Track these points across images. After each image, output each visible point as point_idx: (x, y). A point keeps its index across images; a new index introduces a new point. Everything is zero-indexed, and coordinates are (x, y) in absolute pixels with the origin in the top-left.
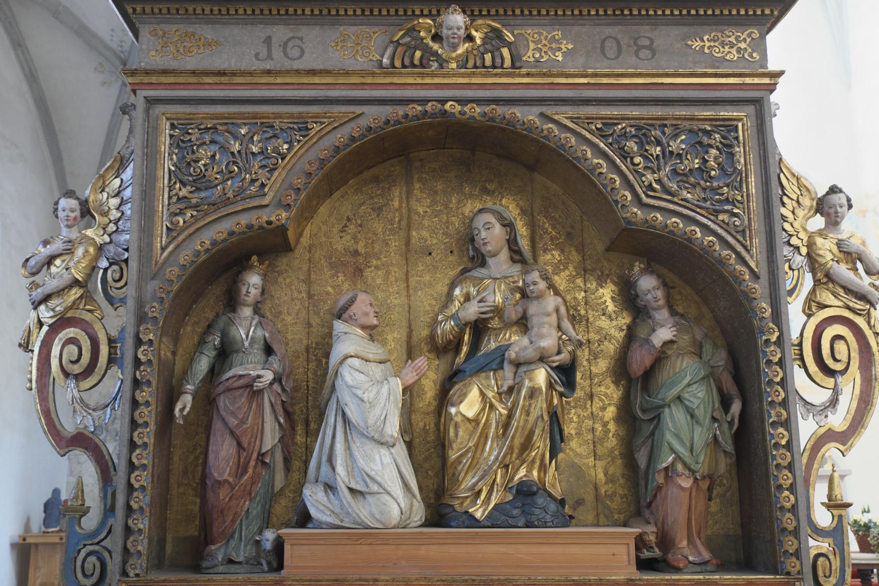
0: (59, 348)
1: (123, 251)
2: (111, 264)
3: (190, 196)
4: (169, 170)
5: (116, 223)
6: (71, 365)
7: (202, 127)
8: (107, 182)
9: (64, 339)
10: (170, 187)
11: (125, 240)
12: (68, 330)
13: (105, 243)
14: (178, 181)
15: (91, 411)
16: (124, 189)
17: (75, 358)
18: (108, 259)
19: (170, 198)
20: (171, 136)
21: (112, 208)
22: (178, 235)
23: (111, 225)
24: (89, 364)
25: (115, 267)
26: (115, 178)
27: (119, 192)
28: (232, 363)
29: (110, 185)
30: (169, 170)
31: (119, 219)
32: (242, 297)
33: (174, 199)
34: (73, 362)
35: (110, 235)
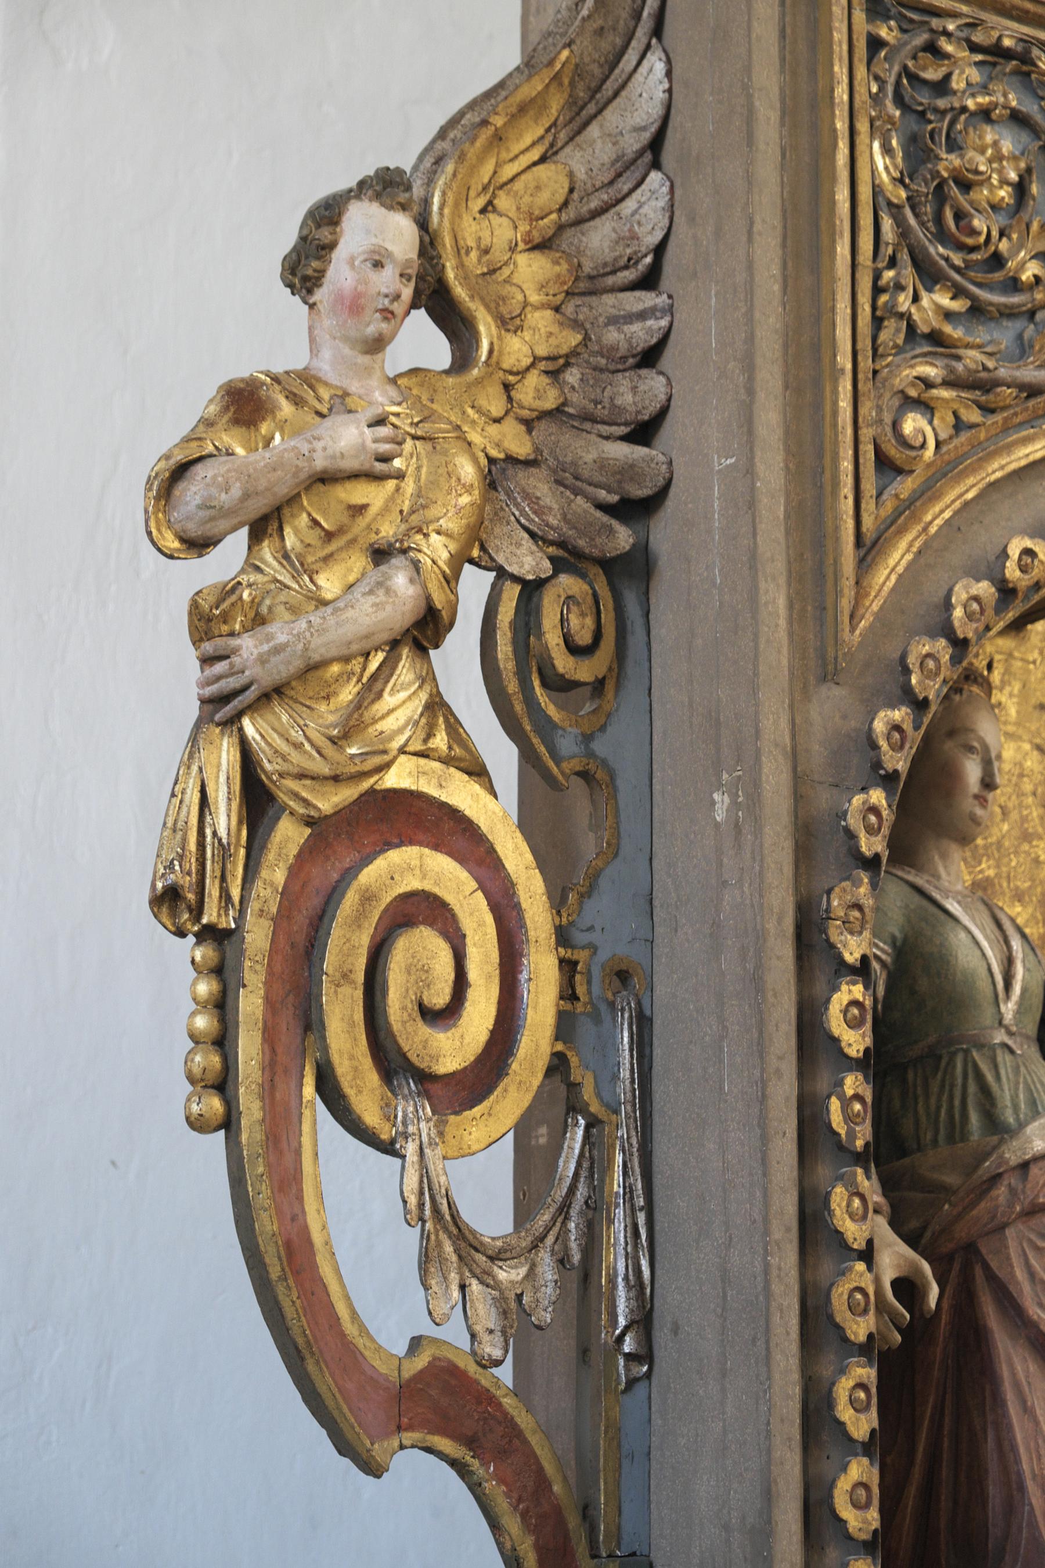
0: (364, 940)
1: (605, 518)
2: (559, 566)
3: (954, 332)
4: (877, 190)
5: (554, 374)
6: (424, 1030)
7: (978, 37)
8: (509, 171)
9: (387, 899)
10: (877, 276)
11: (602, 464)
12: (395, 856)
13: (511, 460)
14: (904, 256)
15: (481, 1258)
16: (579, 222)
17: (440, 997)
18: (532, 535)
19: (878, 322)
20: (875, 44)
21: (534, 298)
22: (927, 493)
23: (533, 379)
24: (493, 1032)
25: (567, 582)
26: (543, 159)
27: (561, 228)
28: (985, 1090)
29: (518, 185)
30: (877, 190)
31: (569, 359)
32: (969, 805)
33: (892, 333)
34: (431, 1016)
35: (528, 424)
